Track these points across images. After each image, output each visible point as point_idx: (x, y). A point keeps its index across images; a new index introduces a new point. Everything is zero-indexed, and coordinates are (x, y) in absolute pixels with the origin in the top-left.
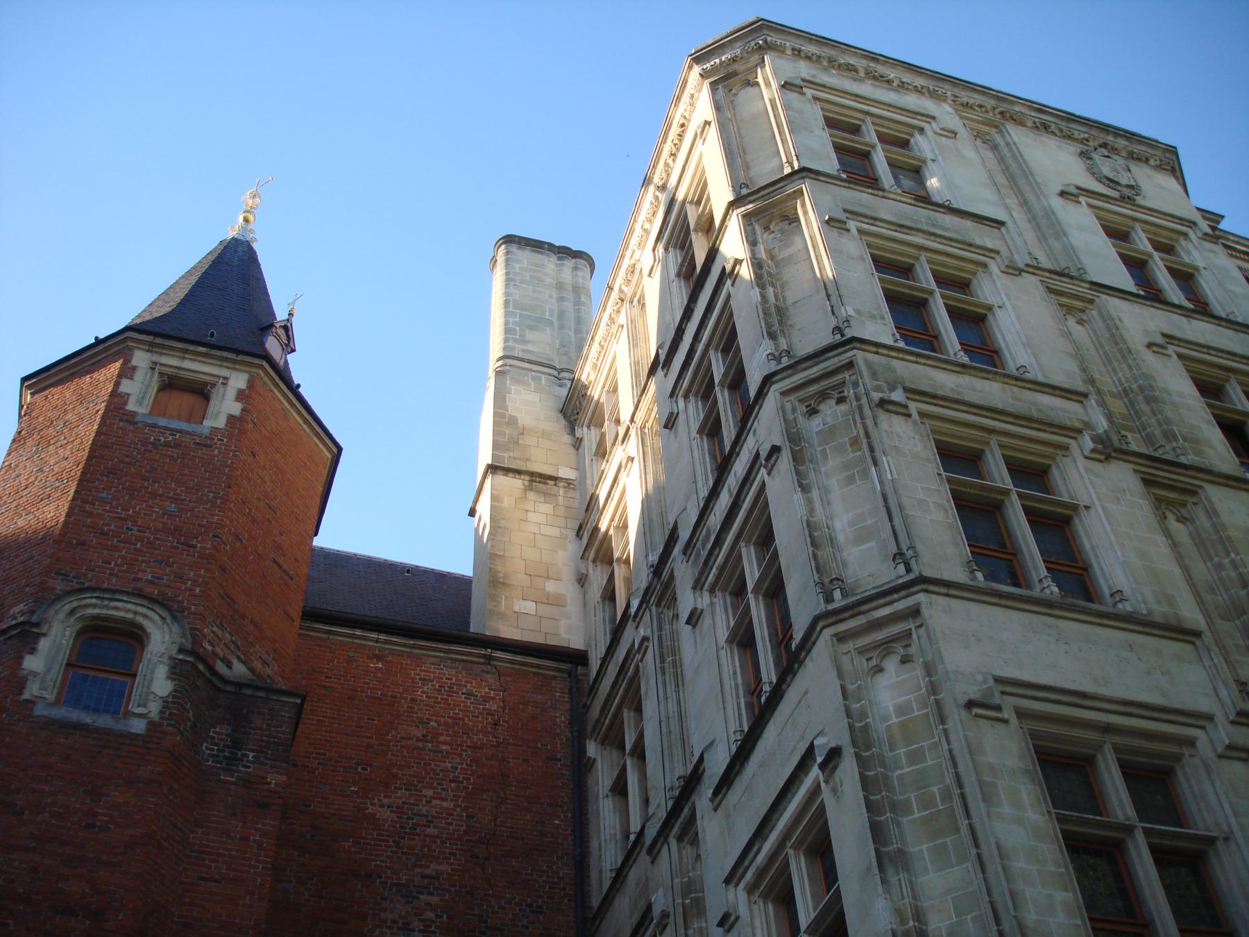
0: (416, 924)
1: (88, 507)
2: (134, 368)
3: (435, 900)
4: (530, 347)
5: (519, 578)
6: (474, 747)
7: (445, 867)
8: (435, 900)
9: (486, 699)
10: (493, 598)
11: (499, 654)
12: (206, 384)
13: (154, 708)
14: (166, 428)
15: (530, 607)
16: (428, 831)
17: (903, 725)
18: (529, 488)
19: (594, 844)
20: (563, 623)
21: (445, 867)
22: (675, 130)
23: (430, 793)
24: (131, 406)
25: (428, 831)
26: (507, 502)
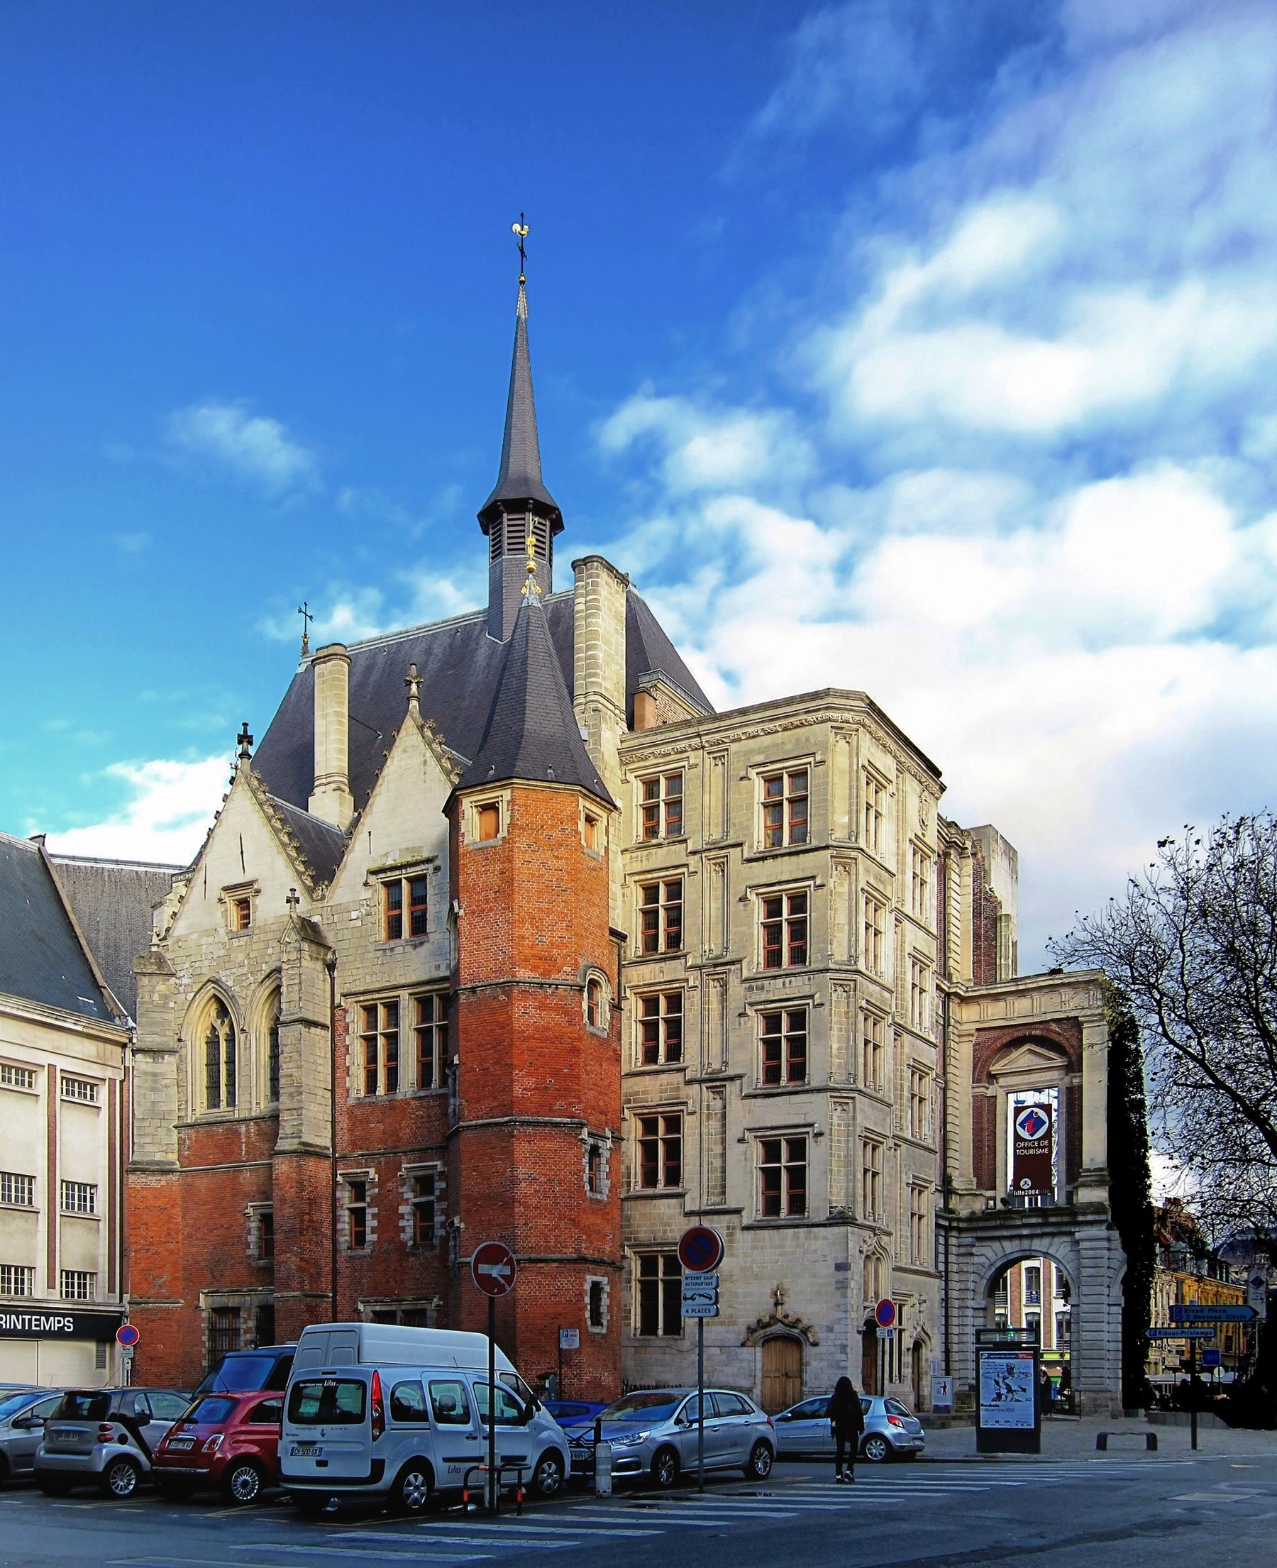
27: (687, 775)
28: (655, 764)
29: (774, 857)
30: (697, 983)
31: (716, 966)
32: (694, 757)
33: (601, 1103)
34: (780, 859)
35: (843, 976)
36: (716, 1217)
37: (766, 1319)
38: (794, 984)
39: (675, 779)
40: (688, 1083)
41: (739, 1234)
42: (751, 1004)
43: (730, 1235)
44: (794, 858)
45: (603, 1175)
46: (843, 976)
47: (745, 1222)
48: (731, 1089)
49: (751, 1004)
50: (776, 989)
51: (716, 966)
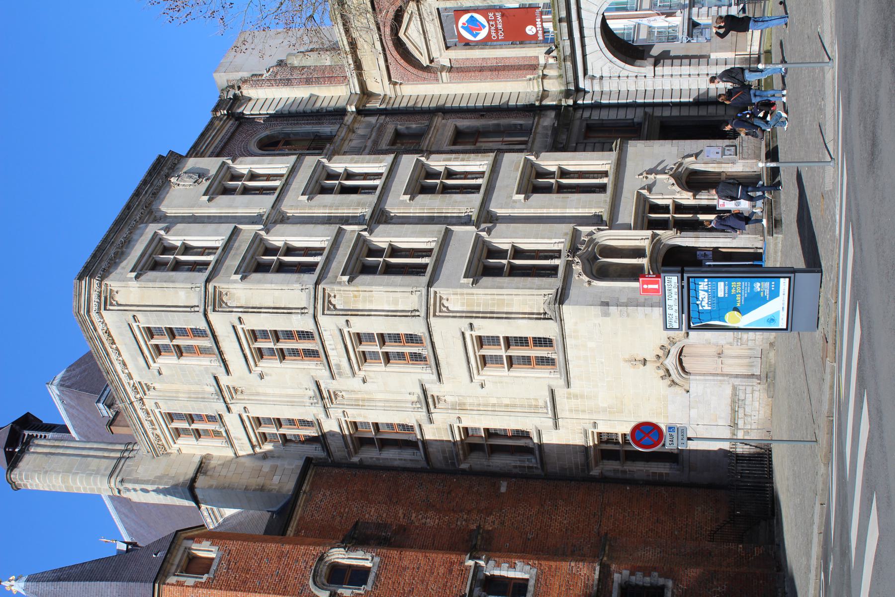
0: (424, 521)
1: (265, 588)
2: (178, 582)
3: (414, 515)
4: (103, 468)
5: (261, 481)
6: (348, 499)
7: (401, 512)
8: (414, 515)
9: (324, 495)
10: (270, 491)
11: (304, 488)
12: (188, 556)
13: (369, 556)
14: (218, 566)
15: (276, 479)
16: (384, 515)
17: (467, 306)
18: (205, 474)
19: (396, 463)
20: (286, 466)
21: (401, 512)
22: (104, 338)
23: (367, 516)
24: (203, 580)
25: (384, 515)
26: (214, 483)
27: (165, 409)
28: (163, 430)
29: (221, 353)
30: (340, 411)
31: (322, 398)
32: (149, 404)
33: (442, 570)
34: (222, 349)
35: (320, 301)
36: (558, 407)
37: (662, 372)
38: (332, 342)
39: (171, 417)
40: (431, 421)
41: (572, 390)
42: (354, 374)
43: (576, 397)
44: (220, 339)
45: (511, 574)
46: (320, 301)
47: (562, 382)
48: (434, 389)
49: (354, 374)
50: (337, 355)
51: (322, 398)
